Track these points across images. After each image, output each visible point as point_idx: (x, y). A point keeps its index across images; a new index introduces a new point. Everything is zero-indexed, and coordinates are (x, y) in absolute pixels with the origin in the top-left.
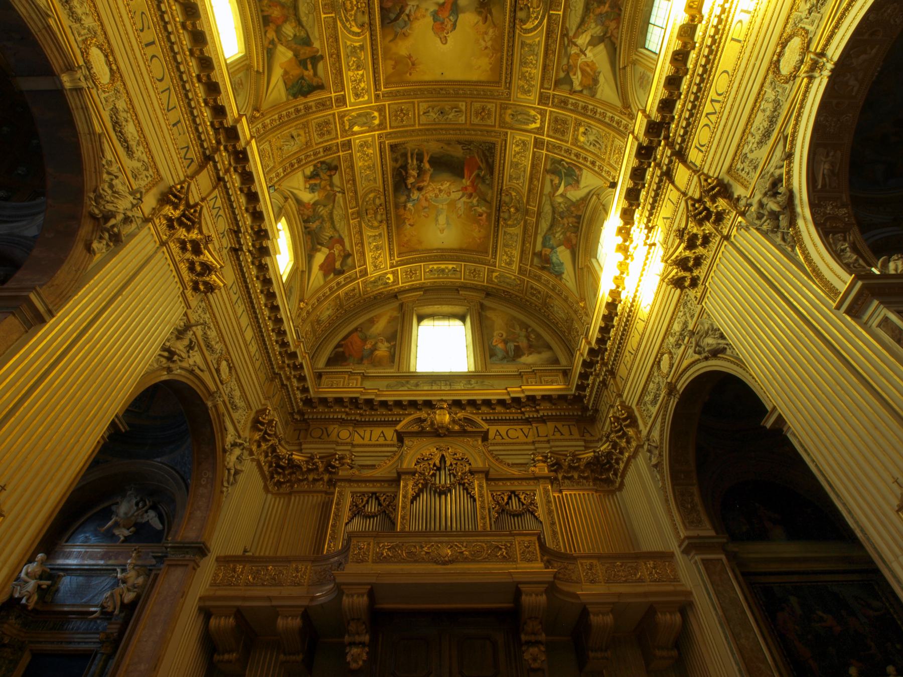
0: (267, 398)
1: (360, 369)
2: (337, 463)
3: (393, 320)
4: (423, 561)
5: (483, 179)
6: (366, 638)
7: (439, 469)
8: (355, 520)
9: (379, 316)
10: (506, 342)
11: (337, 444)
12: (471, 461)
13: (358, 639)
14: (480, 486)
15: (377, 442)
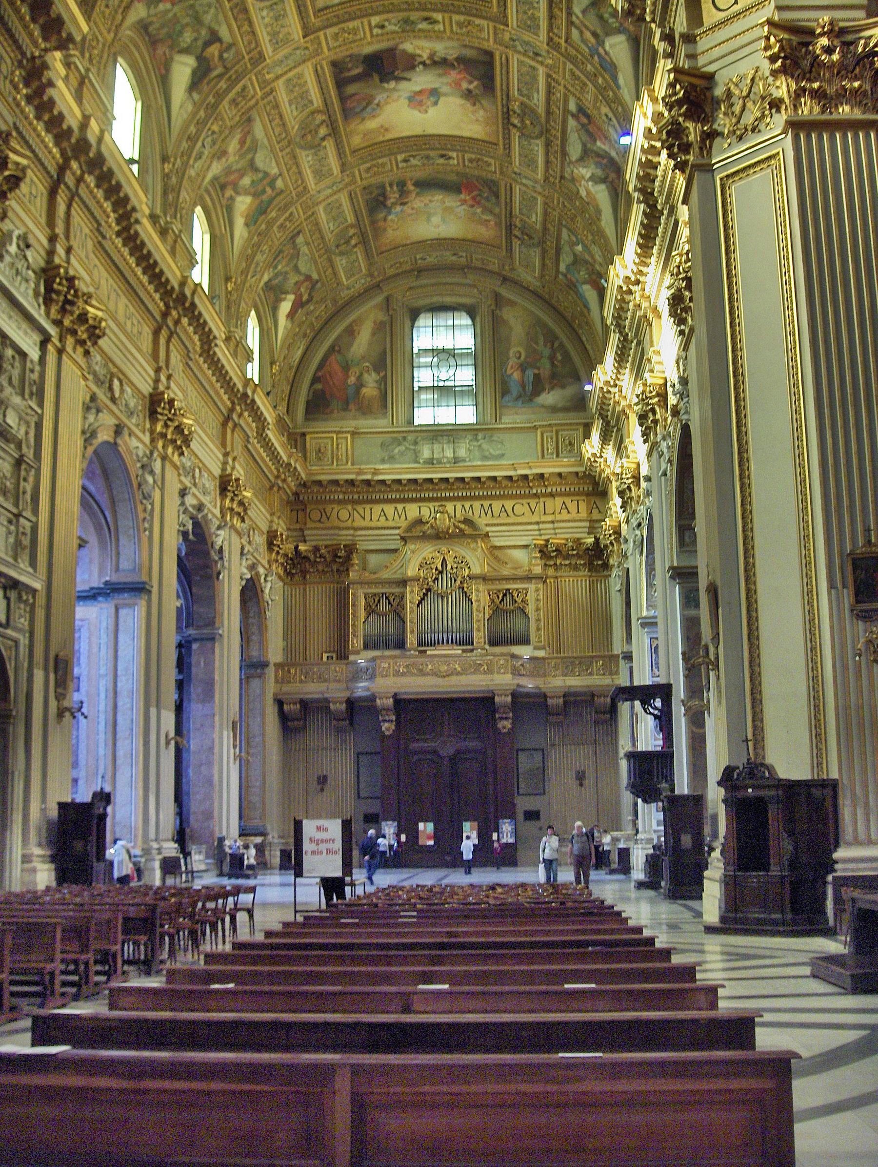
0: (272, 514)
1: (350, 424)
2: (342, 553)
3: (379, 327)
4: (428, 674)
5: (487, 199)
6: (394, 718)
7: (441, 572)
8: (371, 619)
9: (359, 321)
10: (523, 368)
11: (339, 528)
12: (471, 564)
13: (387, 718)
14: (477, 590)
15: (379, 524)
